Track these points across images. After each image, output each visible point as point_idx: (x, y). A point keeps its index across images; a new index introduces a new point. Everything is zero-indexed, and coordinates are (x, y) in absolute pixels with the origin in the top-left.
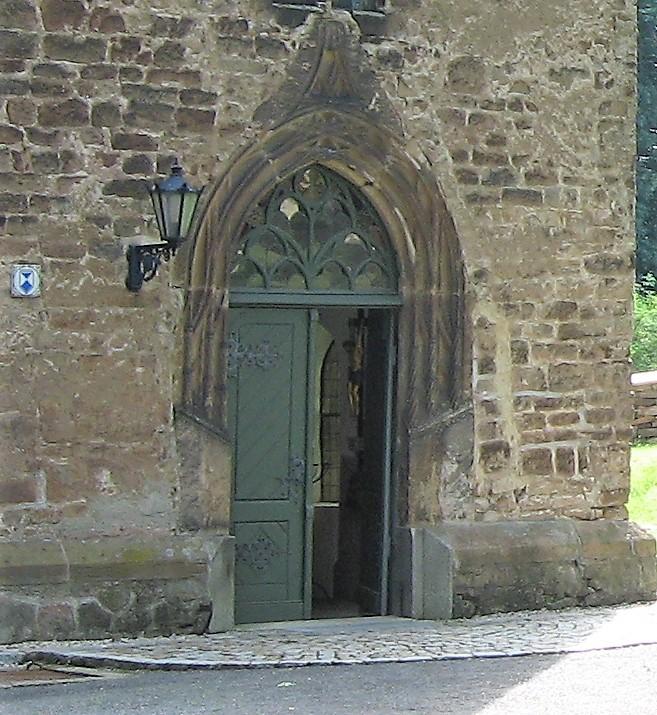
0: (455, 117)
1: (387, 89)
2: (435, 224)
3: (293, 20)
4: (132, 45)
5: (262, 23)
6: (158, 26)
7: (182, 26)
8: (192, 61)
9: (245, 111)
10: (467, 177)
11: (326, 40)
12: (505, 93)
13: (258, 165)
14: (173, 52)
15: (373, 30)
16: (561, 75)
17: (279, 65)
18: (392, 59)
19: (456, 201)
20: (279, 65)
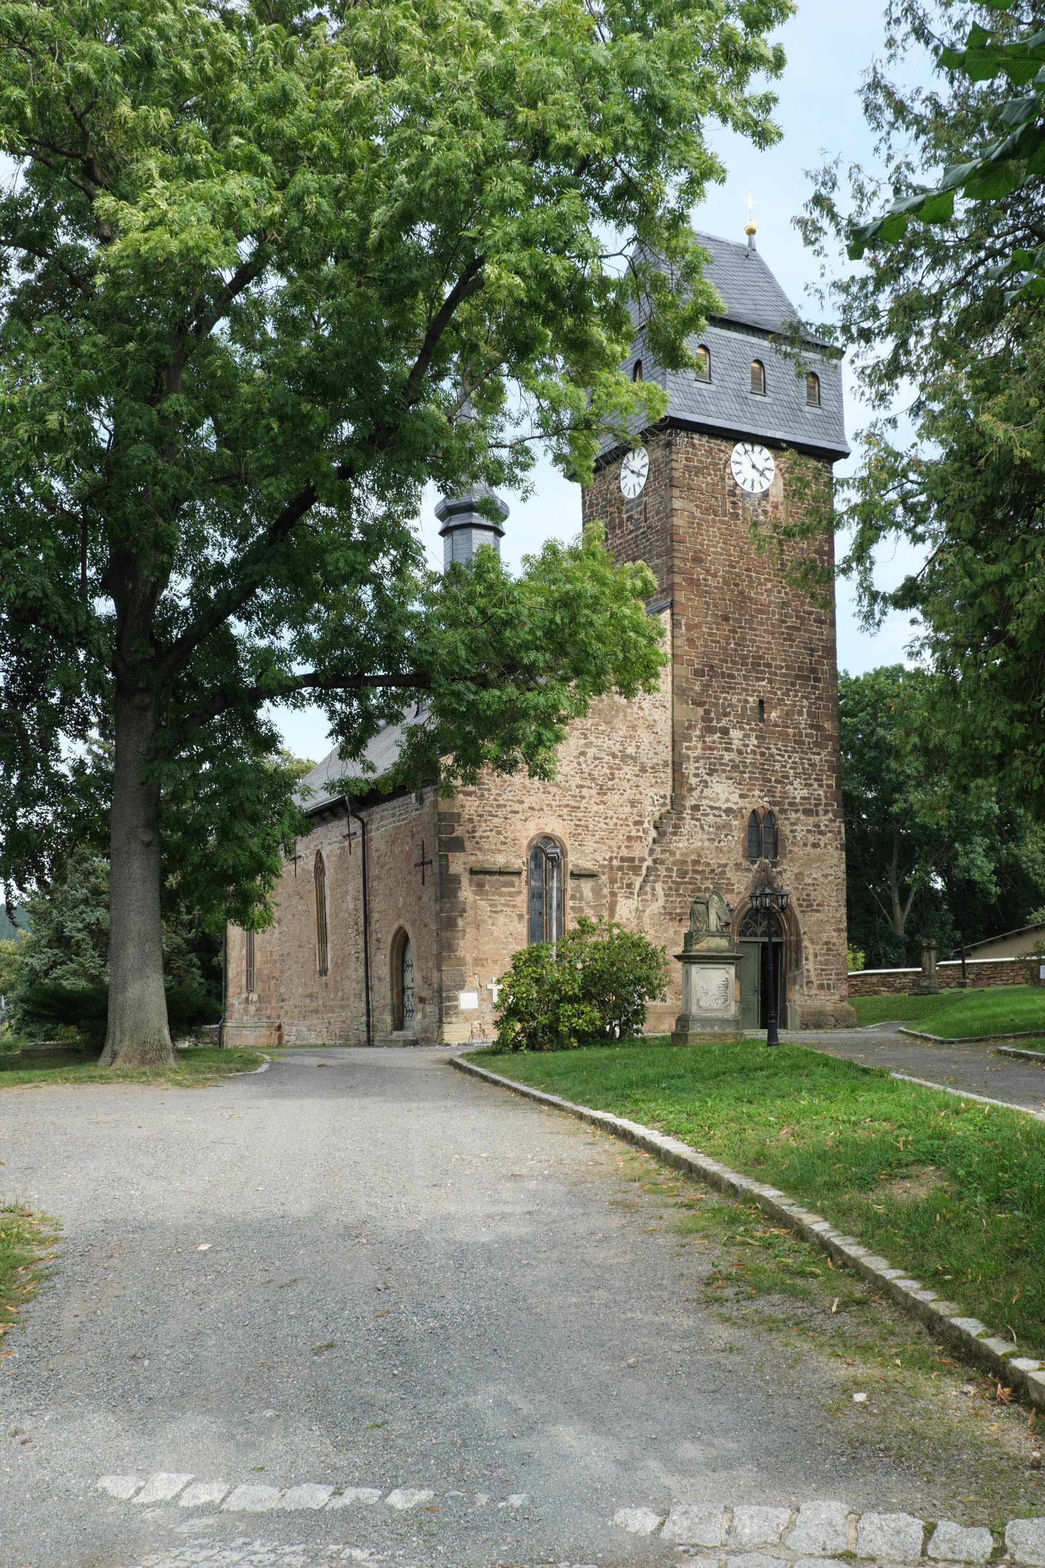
0: (796, 889)
1: (779, 882)
2: (793, 920)
3: (753, 863)
4: (713, 871)
5: (746, 864)
6: (720, 866)
7: (725, 866)
8: (728, 875)
9: (742, 888)
10: (801, 906)
11: (763, 869)
12: (810, 881)
13: (746, 903)
14: (723, 873)
15: (775, 865)
16: (825, 876)
17: (750, 875)
18: (780, 873)
19: (799, 916)
20: (750, 875)
